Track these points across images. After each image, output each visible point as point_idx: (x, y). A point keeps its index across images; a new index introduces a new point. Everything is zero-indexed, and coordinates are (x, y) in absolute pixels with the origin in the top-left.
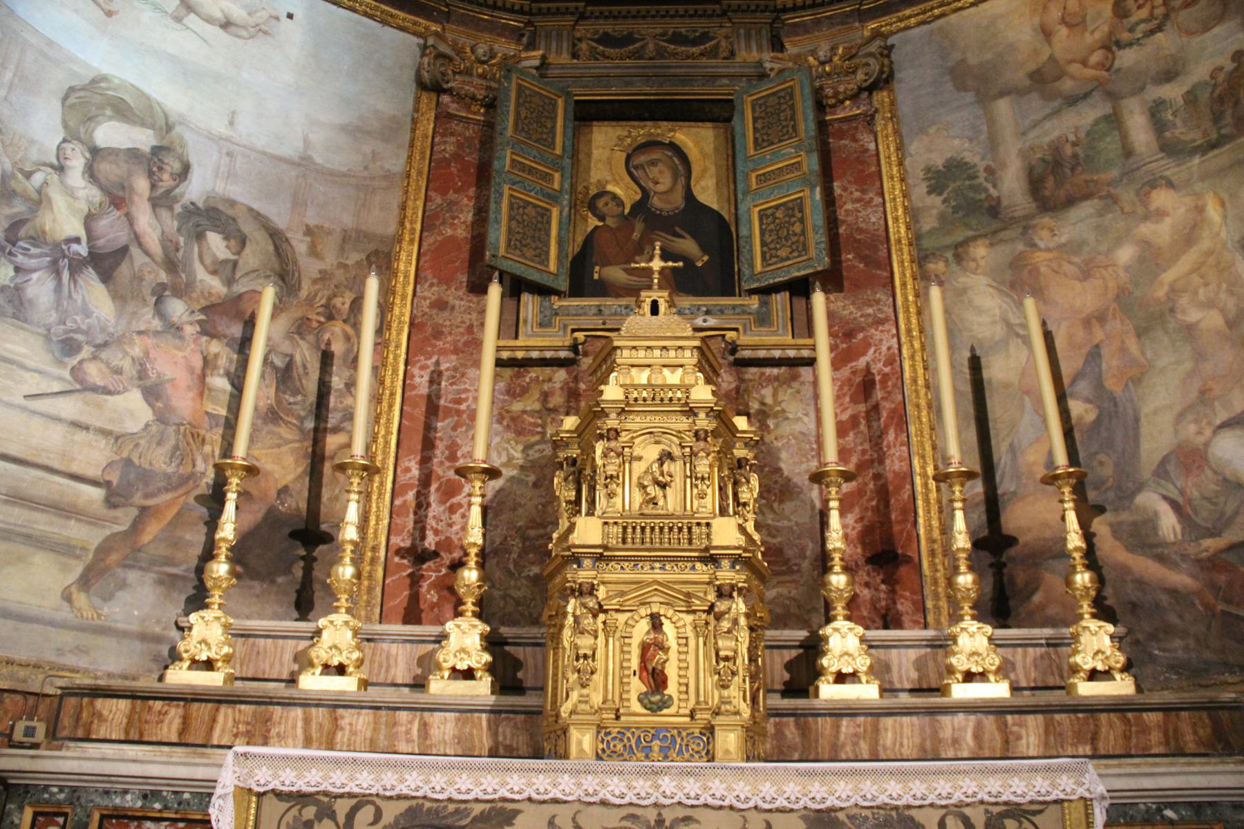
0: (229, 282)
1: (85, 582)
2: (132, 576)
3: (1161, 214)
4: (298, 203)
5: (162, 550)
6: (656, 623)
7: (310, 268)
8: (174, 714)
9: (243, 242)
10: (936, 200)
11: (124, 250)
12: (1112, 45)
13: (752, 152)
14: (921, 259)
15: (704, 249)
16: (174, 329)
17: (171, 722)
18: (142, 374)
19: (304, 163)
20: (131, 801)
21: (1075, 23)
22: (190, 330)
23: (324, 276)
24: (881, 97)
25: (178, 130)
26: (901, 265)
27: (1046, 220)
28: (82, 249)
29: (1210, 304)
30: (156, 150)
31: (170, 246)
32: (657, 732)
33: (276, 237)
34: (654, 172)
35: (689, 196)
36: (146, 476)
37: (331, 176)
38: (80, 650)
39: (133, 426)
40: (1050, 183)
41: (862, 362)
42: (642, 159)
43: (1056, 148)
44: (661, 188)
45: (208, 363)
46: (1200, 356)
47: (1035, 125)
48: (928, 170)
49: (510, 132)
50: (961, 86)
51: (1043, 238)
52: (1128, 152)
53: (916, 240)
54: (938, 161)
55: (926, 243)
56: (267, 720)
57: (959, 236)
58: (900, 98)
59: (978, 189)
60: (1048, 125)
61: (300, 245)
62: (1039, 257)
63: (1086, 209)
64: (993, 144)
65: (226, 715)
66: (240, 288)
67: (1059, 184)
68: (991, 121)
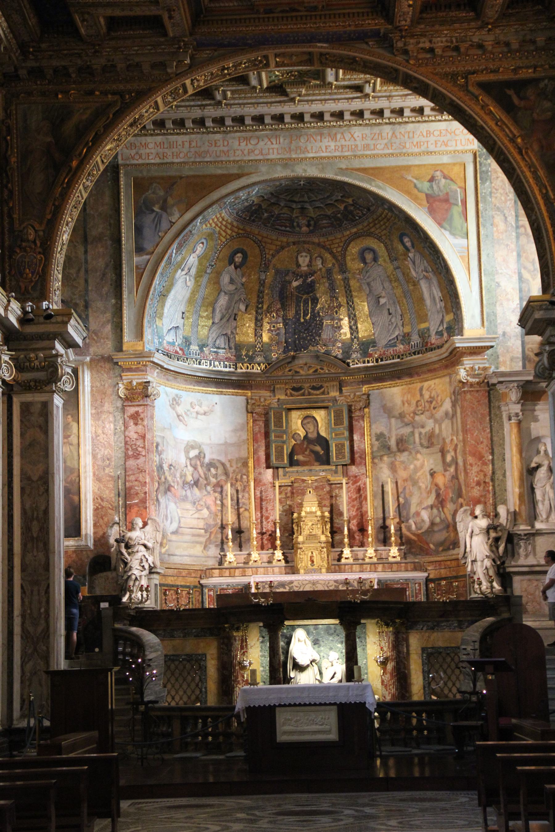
0: (216, 479)
1: (205, 548)
2: (211, 546)
3: (417, 459)
4: (226, 455)
5: (214, 540)
6: (312, 553)
7: (231, 470)
8: (228, 571)
9: (217, 468)
10: (377, 443)
12: (415, 413)
13: (333, 426)
14: (373, 458)
15: (323, 450)
16: (209, 493)
17: (227, 573)
18: (206, 504)
19: (226, 444)
20: (225, 587)
21: (409, 404)
22: (212, 492)
23: (234, 471)
24: (366, 410)
26: (368, 459)
27: (398, 454)
28: (192, 482)
29: (423, 483)
30: (199, 453)
31: (205, 474)
32: (313, 569)
33: (223, 464)
34: (309, 426)
35: (318, 433)
36: (210, 525)
37: (232, 445)
38: (206, 561)
39: (206, 516)
40: (400, 445)
41: (358, 484)
42: (305, 421)
43: (402, 436)
44: (311, 431)
45: (216, 498)
46: (421, 493)
47: (399, 428)
48: (376, 434)
49: (273, 428)
50: (385, 412)
51: (398, 458)
52: (415, 443)
53: (372, 453)
54: (378, 432)
55: (374, 454)
56: (245, 571)
57: (382, 453)
58: (371, 411)
59: (386, 442)
60: (401, 429)
61: (228, 465)
62: (397, 463)
63: (406, 453)
64: (390, 431)
65: (237, 571)
66: (219, 479)
67: (402, 445)
68: (390, 424)
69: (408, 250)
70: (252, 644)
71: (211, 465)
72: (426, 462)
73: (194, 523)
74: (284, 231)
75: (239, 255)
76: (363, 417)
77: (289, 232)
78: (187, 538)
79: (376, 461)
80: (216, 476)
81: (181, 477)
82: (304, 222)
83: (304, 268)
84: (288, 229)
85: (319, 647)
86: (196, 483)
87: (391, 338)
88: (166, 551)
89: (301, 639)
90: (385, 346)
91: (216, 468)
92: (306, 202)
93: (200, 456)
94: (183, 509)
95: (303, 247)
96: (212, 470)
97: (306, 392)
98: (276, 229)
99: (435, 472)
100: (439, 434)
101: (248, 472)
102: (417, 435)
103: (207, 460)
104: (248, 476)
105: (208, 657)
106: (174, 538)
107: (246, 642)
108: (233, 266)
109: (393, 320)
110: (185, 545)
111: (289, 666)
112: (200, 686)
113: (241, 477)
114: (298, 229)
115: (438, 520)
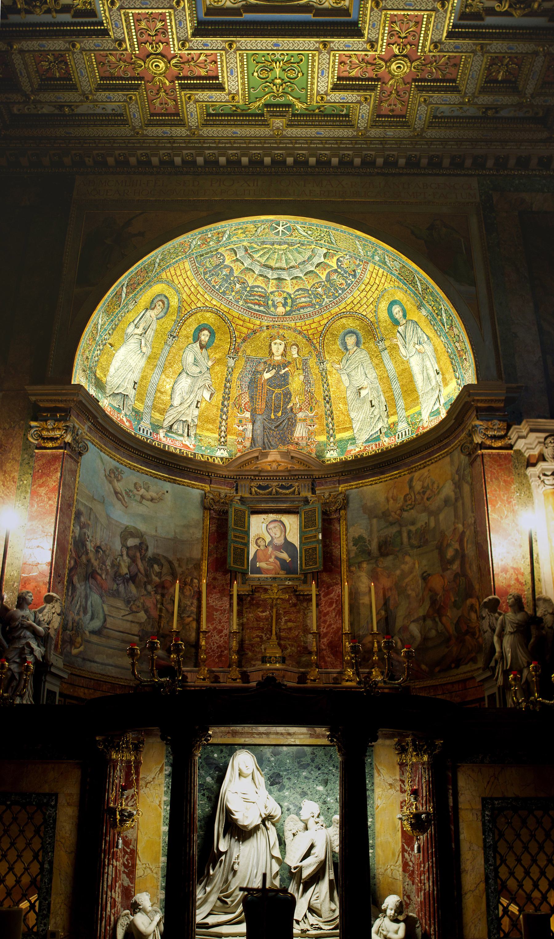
11: (137, 574)
25: (144, 536)
69: (396, 323)
70: (149, 778)
71: (155, 560)
72: (417, 566)
73: (125, 626)
74: (258, 311)
75: (206, 332)
76: (339, 520)
77: (264, 312)
78: (116, 643)
79: (353, 569)
80: (159, 575)
81: (113, 565)
82: (281, 299)
83: (278, 358)
84: (262, 308)
85: (279, 790)
86: (133, 578)
87: (373, 432)
88: (80, 653)
89: (245, 771)
90: (367, 441)
91: (161, 565)
92: (284, 269)
93: (142, 547)
94: (112, 606)
95: (278, 333)
96: (156, 567)
97: (274, 490)
98: (248, 307)
99: (429, 575)
100: (434, 528)
101: (200, 576)
102: (405, 535)
103: (150, 553)
104: (200, 581)
105: (62, 800)
106: (94, 639)
107: (137, 773)
108: (198, 344)
109: (376, 413)
110: (110, 651)
111: (218, 827)
112: (40, 858)
113: (192, 580)
114: (272, 309)
115: (433, 633)
